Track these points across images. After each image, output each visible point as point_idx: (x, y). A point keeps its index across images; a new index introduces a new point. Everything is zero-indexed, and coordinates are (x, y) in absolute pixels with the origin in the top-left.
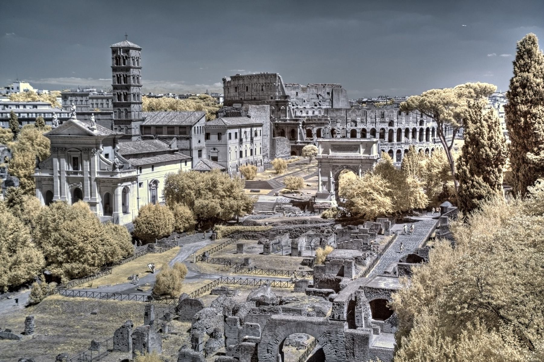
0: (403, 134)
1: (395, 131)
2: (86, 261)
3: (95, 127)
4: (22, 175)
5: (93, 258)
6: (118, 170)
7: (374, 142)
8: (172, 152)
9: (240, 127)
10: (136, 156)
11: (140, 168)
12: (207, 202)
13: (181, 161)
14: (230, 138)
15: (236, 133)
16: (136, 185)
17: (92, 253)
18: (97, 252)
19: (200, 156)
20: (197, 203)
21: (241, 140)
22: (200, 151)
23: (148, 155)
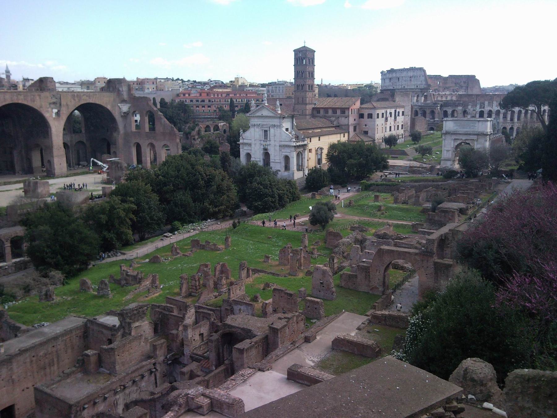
14: (378, 117)
15: (383, 114)
19: (355, 130)
21: (386, 119)
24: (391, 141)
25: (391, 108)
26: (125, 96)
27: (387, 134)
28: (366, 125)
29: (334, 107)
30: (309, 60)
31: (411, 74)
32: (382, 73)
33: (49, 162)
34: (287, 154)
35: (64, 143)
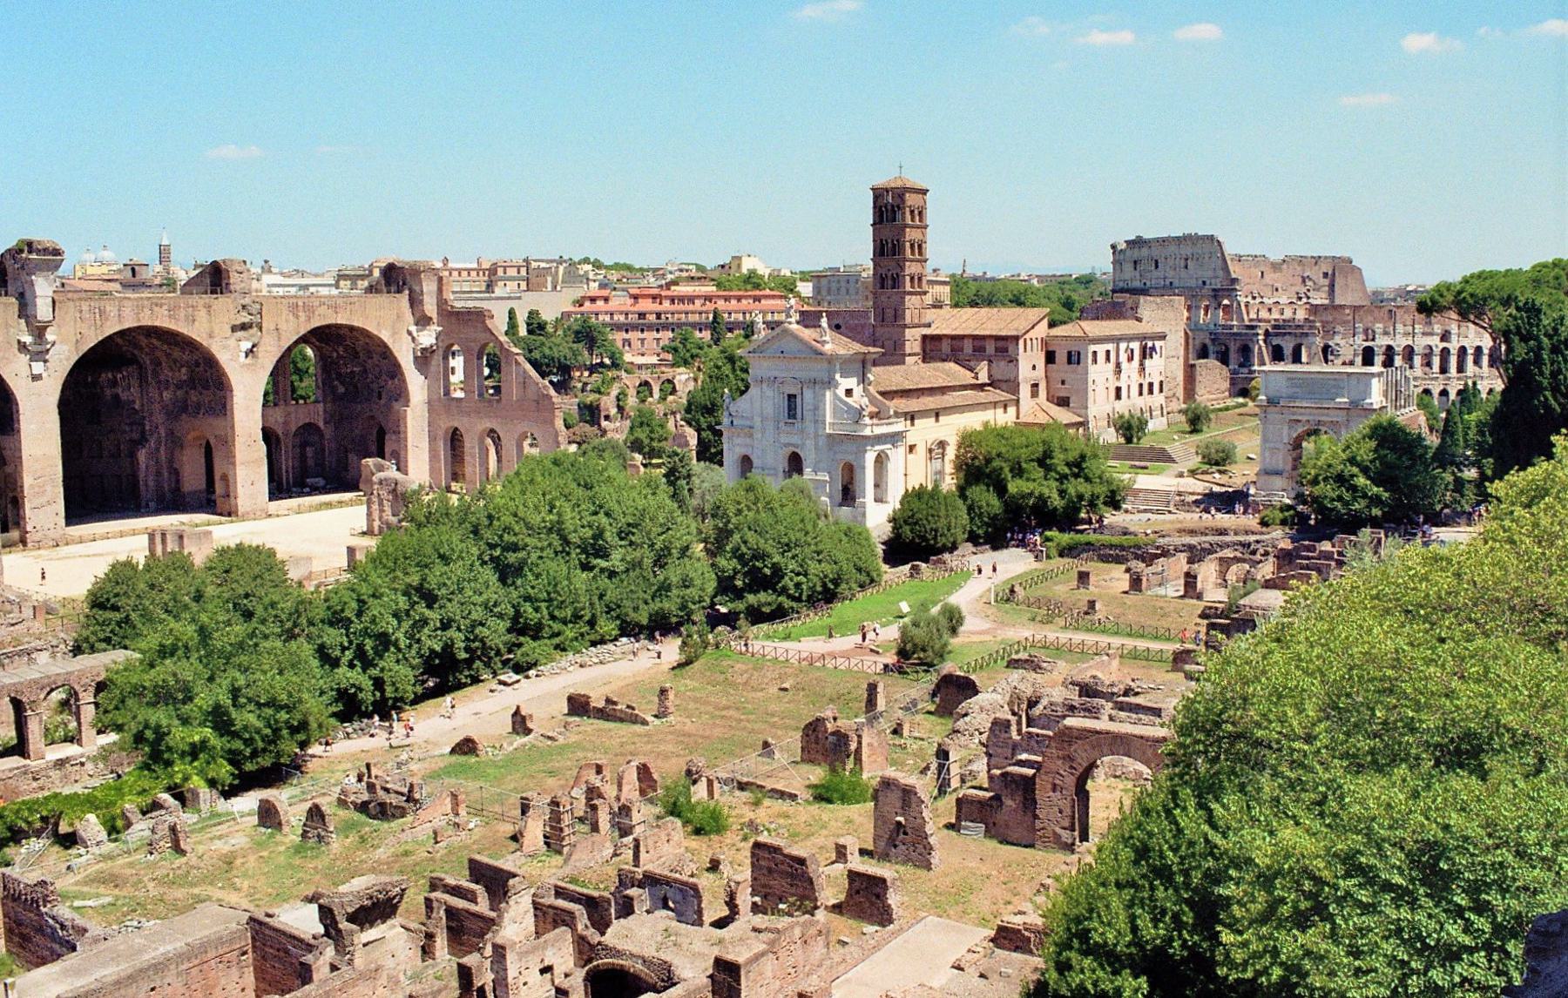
0: (1470, 359)
1: (1454, 351)
2: (784, 590)
3: (827, 338)
4: (704, 426)
5: (798, 585)
6: (867, 420)
7: (1373, 375)
8: (981, 387)
9: (1117, 340)
10: (905, 393)
11: (912, 417)
12: (1031, 485)
13: (995, 405)
14: (1095, 361)
15: (1108, 352)
16: (902, 450)
17: (798, 574)
18: (806, 575)
19: (1035, 394)
20: (1014, 487)
21: (1118, 365)
22: (1035, 386)
23: (931, 391)
24: (1130, 429)
25: (1130, 339)
26: (430, 308)
27: (1122, 407)
28: (1063, 383)
29: (976, 333)
30: (912, 212)
31: (1186, 250)
32: (1113, 247)
33: (225, 478)
34: (850, 458)
35: (263, 429)
